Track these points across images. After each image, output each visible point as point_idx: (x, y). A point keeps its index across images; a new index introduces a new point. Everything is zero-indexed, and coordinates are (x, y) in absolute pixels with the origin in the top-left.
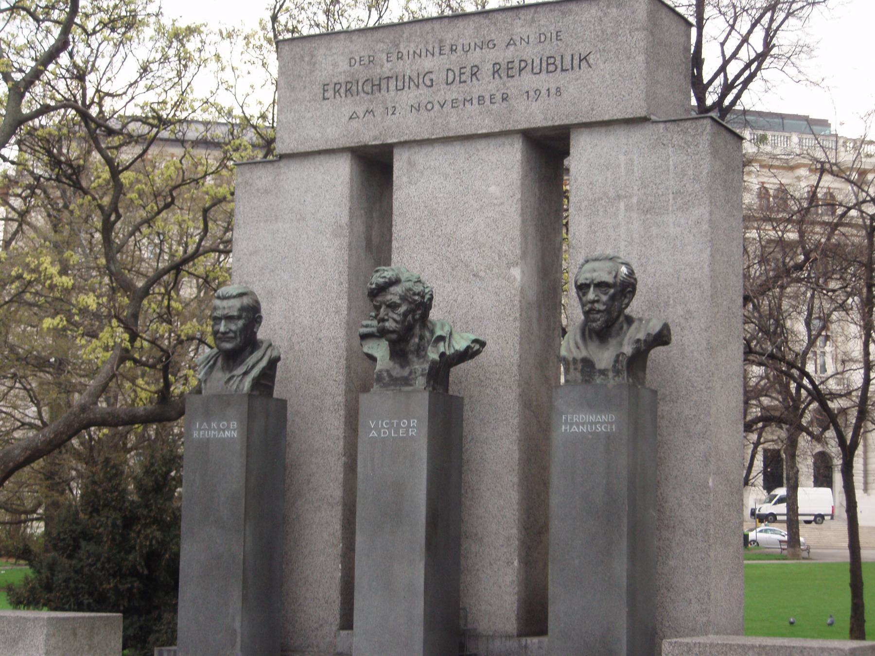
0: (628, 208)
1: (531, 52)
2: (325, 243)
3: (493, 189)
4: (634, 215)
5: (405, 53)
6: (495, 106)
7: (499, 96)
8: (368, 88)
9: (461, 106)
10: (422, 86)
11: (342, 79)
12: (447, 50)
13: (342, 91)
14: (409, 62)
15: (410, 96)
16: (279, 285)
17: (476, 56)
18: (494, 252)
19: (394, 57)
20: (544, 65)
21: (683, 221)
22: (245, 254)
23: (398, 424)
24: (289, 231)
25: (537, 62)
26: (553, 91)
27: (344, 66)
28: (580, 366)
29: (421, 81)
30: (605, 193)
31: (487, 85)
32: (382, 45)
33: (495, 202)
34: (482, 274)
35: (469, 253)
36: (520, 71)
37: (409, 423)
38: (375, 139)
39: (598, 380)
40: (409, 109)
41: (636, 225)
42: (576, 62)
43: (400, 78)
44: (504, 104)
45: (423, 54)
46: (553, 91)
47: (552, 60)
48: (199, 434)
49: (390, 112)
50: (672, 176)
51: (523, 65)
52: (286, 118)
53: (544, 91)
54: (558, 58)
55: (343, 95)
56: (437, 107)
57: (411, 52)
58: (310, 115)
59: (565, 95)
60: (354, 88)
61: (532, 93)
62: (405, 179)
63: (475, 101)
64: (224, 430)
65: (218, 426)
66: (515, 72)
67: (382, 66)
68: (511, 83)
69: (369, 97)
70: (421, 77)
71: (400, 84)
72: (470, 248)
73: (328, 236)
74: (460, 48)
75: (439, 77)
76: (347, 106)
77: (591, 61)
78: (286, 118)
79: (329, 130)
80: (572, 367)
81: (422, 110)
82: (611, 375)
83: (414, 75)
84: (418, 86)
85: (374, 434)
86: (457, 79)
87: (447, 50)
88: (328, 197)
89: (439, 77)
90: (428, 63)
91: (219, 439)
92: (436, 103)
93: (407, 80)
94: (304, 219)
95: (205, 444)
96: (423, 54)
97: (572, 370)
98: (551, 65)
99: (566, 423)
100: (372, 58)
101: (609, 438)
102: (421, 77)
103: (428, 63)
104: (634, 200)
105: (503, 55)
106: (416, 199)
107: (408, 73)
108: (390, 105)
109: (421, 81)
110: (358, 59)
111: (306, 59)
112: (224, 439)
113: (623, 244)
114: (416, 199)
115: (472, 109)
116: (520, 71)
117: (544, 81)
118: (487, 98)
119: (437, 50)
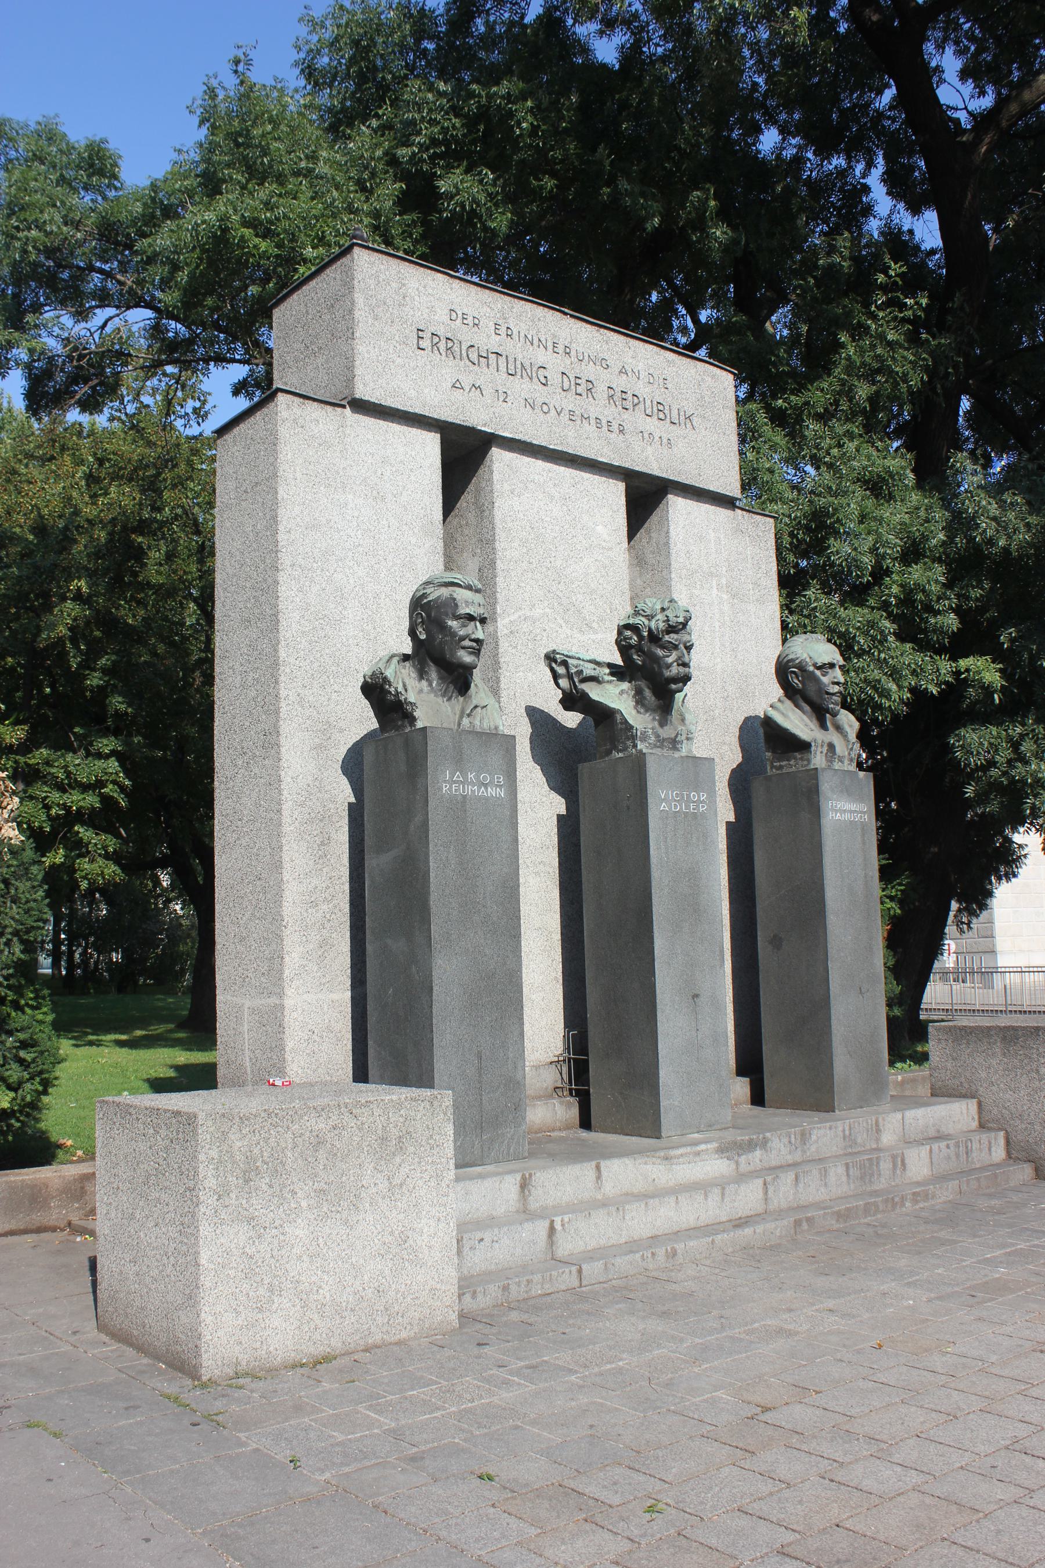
0: (719, 587)
1: (643, 390)
2: (413, 540)
3: (600, 529)
4: (725, 597)
5: (515, 332)
6: (613, 436)
7: (615, 427)
8: (474, 356)
9: (579, 422)
10: (535, 380)
11: (441, 332)
12: (560, 349)
13: (442, 346)
14: (519, 345)
15: (521, 387)
16: (351, 581)
17: (589, 371)
18: (605, 602)
19: (503, 331)
20: (655, 409)
21: (761, 615)
22: (297, 525)
23: (688, 796)
24: (363, 510)
25: (648, 403)
26: (665, 441)
27: (442, 315)
28: (825, 748)
29: (534, 375)
30: (700, 567)
31: (599, 407)
32: (489, 310)
33: (604, 544)
34: (595, 625)
35: (580, 597)
36: (635, 406)
37: (699, 796)
38: (485, 425)
39: (837, 765)
40: (523, 402)
41: (726, 608)
42: (682, 418)
43: (511, 360)
44: (621, 436)
45: (536, 342)
46: (665, 441)
47: (661, 408)
48: (450, 789)
49: (501, 399)
50: (749, 566)
51: (636, 400)
52: (368, 352)
53: (657, 438)
54: (667, 408)
55: (444, 354)
56: (553, 412)
57: (522, 335)
58: (399, 361)
59: (675, 449)
60: (456, 348)
61: (646, 435)
62: (506, 486)
63: (593, 421)
64: (486, 786)
65: (477, 777)
66: (628, 404)
67: (488, 336)
68: (626, 415)
69: (476, 368)
70: (534, 369)
71: (511, 367)
72: (582, 591)
73: (416, 531)
74: (573, 353)
75: (555, 378)
76: (449, 370)
77: (694, 423)
78: (368, 352)
79: (426, 391)
80: (819, 749)
81: (538, 410)
82: (846, 762)
83: (527, 365)
84: (531, 379)
85: (663, 806)
86: (573, 387)
87: (560, 349)
88: (412, 478)
89: (555, 378)
90: (542, 357)
91: (480, 799)
92: (551, 406)
93: (519, 366)
94: (383, 499)
95: (460, 805)
96: (536, 342)
97: (818, 753)
98: (660, 411)
99: (832, 810)
100: (476, 321)
101: (863, 826)
102: (534, 369)
103: (542, 357)
104: (724, 581)
105: (620, 383)
106: (521, 515)
107: (520, 357)
108: (501, 390)
109: (534, 375)
110: (460, 313)
111: (394, 285)
112: (487, 799)
113: (717, 624)
114: (521, 515)
115: (590, 428)
116: (635, 406)
117: (651, 425)
118: (604, 422)
119: (550, 345)
